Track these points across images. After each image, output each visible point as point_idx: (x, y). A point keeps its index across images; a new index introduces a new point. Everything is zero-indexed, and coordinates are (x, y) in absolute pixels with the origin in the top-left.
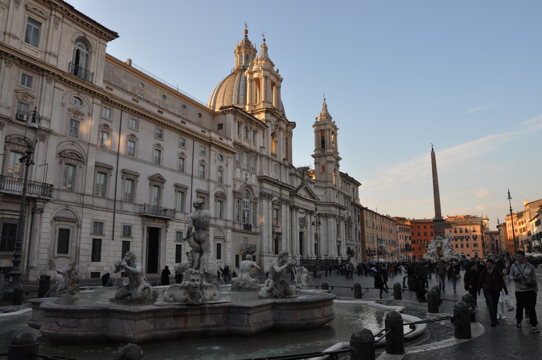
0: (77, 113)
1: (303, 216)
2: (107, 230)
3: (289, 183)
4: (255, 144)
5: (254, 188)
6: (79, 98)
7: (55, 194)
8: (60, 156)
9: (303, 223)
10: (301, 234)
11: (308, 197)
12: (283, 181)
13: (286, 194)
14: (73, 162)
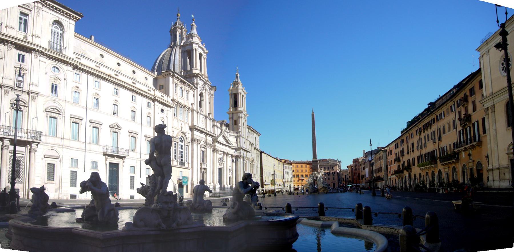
0: (57, 78)
1: (221, 156)
2: (81, 164)
3: (212, 132)
4: (188, 103)
5: (187, 134)
6: (57, 68)
7: (43, 139)
8: (46, 111)
9: (221, 160)
10: (220, 170)
11: (225, 143)
12: (208, 130)
13: (210, 139)
14: (55, 115)
